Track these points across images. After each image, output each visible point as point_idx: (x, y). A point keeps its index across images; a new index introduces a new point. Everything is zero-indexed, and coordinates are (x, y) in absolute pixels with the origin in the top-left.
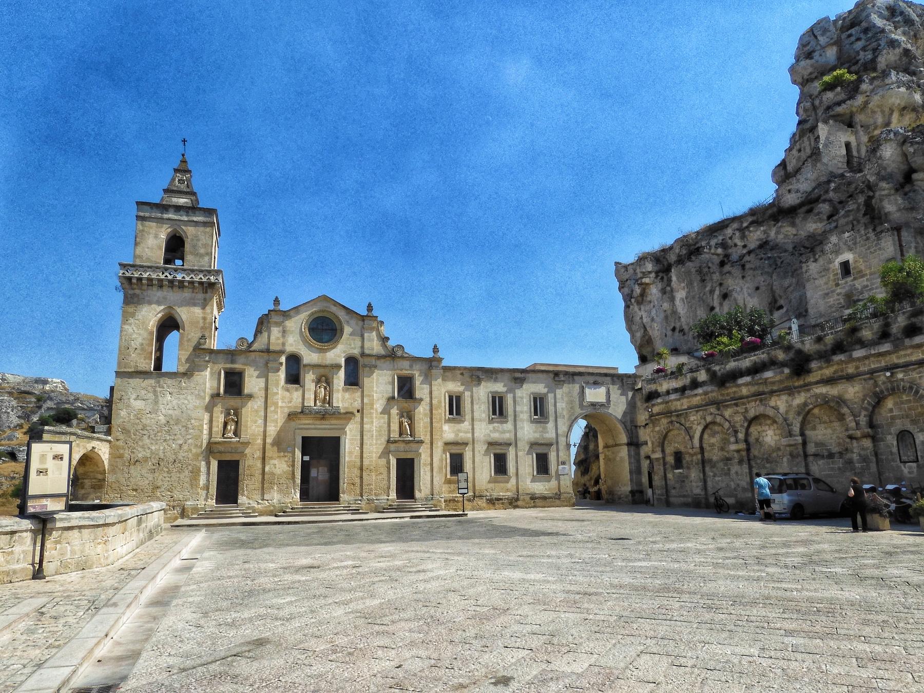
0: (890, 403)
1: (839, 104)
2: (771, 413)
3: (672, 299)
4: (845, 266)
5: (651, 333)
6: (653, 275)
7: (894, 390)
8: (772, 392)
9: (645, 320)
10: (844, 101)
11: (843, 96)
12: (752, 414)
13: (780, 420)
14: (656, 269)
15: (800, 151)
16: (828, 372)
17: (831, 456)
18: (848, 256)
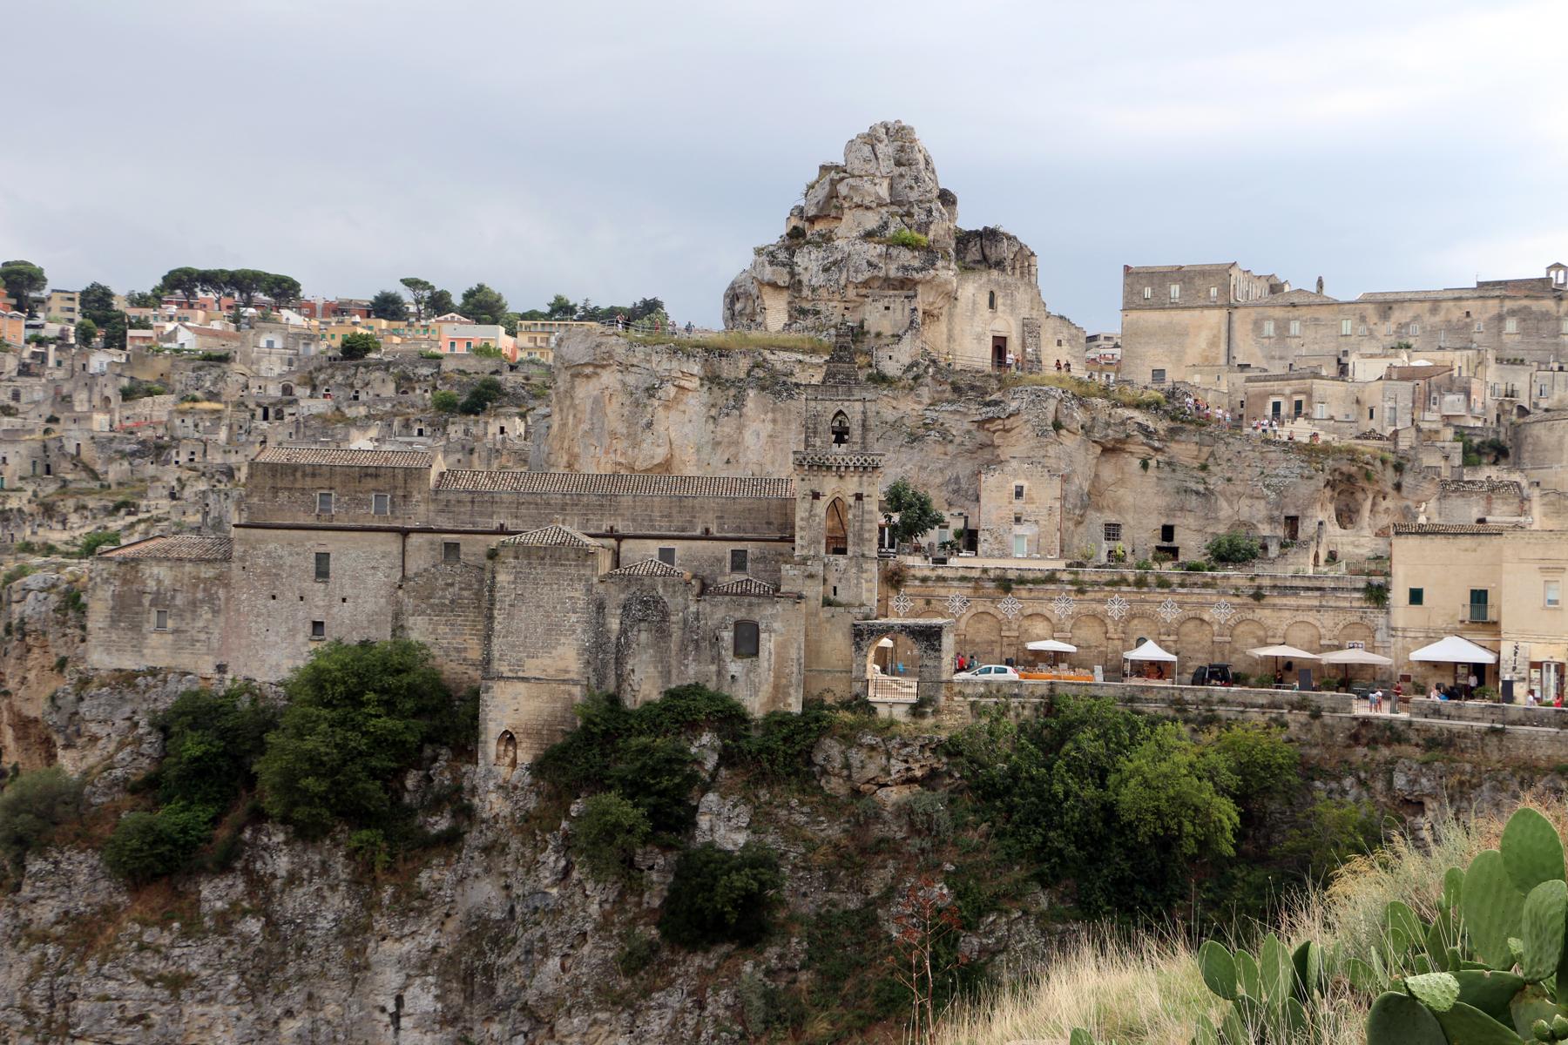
0: (1136, 622)
1: (917, 270)
2: (1048, 614)
3: (740, 429)
4: (1019, 493)
5: (677, 453)
6: (696, 383)
7: (1142, 616)
8: (1051, 600)
9: (672, 435)
10: (922, 269)
11: (916, 263)
12: (1029, 611)
13: (1054, 620)
14: (702, 374)
15: (887, 308)
16: (1100, 595)
17: (1089, 647)
18: (1026, 484)
